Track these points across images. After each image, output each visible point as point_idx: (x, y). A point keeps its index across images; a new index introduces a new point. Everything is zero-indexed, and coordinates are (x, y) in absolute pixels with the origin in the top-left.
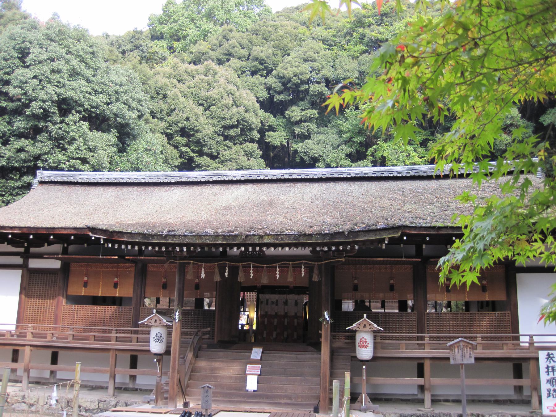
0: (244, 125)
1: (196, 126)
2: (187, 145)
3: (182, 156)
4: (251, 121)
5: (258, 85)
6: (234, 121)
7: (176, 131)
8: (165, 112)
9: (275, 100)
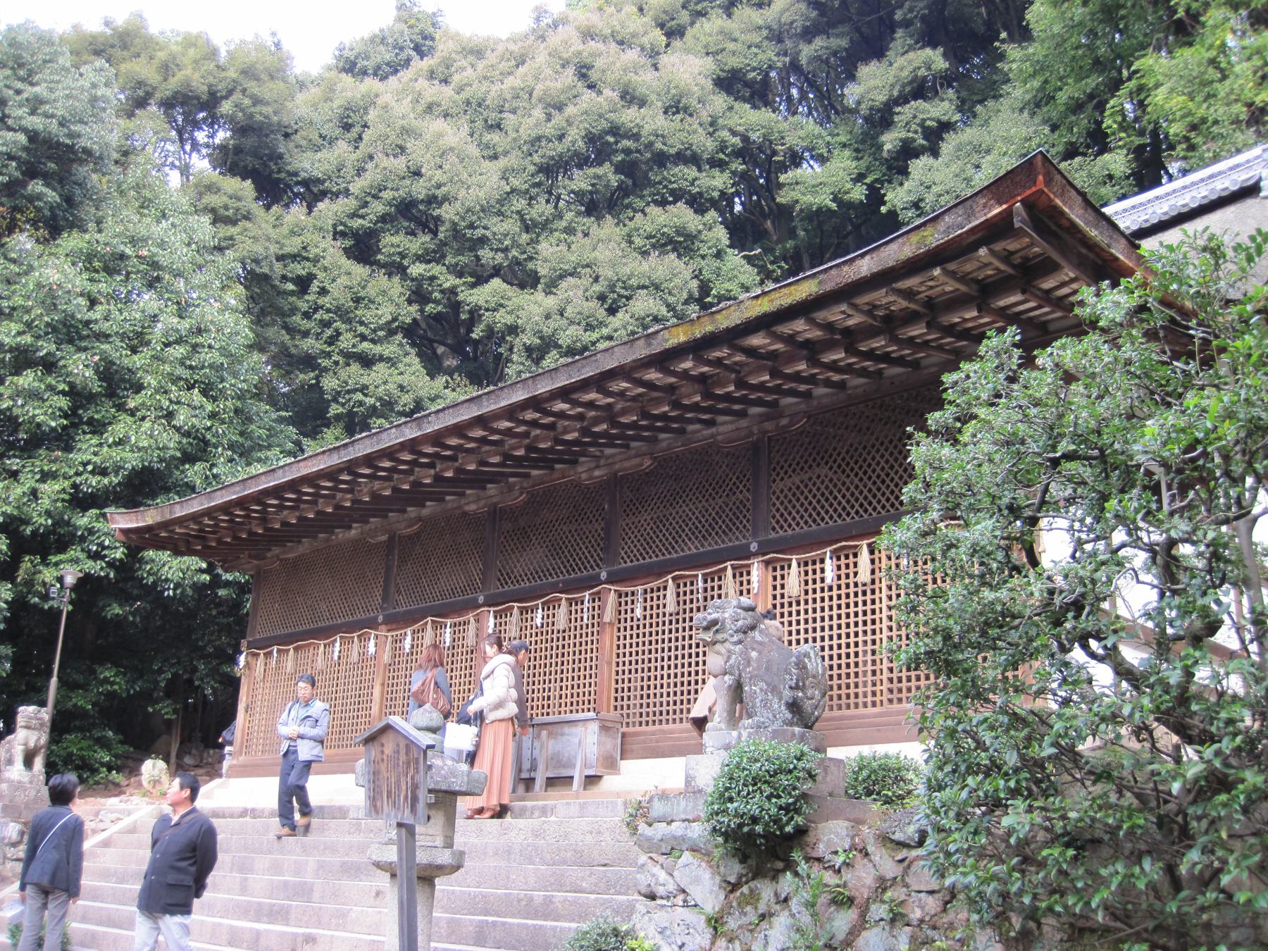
0: (627, 151)
1: (439, 186)
2: (425, 257)
3: (419, 296)
4: (647, 129)
5: (737, 34)
6: (575, 139)
7: (383, 218)
8: (349, 171)
9: (803, 61)
